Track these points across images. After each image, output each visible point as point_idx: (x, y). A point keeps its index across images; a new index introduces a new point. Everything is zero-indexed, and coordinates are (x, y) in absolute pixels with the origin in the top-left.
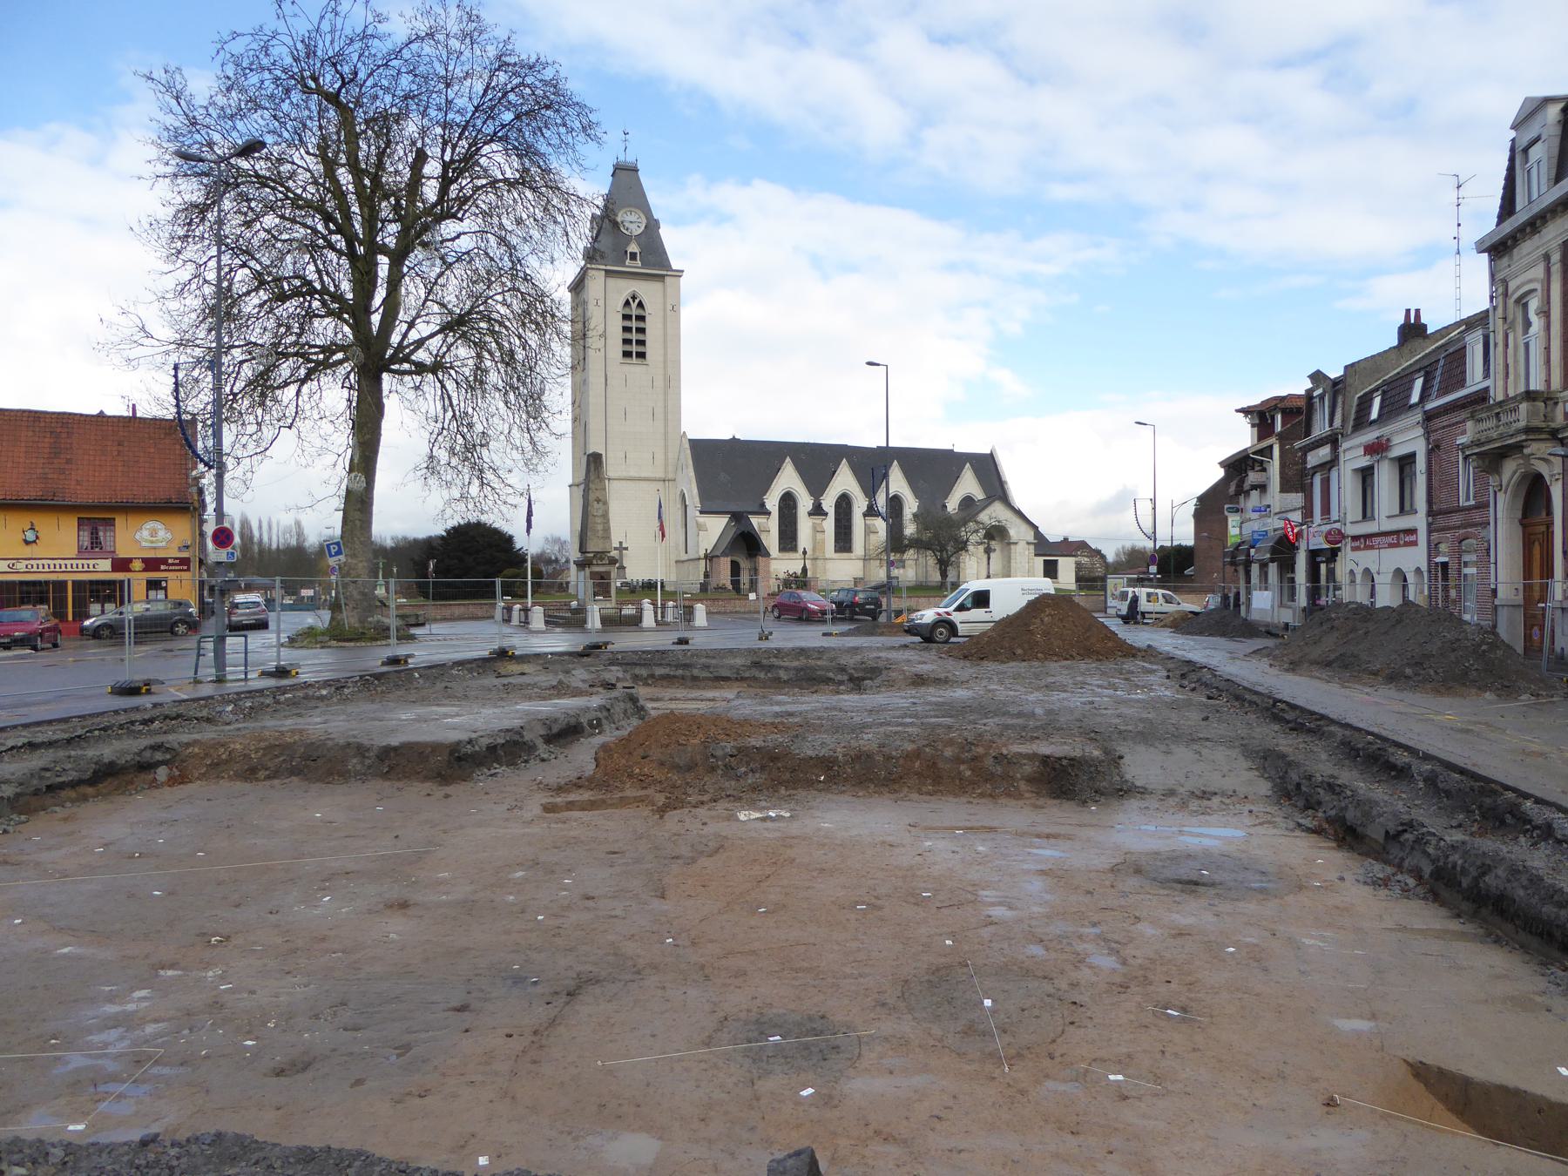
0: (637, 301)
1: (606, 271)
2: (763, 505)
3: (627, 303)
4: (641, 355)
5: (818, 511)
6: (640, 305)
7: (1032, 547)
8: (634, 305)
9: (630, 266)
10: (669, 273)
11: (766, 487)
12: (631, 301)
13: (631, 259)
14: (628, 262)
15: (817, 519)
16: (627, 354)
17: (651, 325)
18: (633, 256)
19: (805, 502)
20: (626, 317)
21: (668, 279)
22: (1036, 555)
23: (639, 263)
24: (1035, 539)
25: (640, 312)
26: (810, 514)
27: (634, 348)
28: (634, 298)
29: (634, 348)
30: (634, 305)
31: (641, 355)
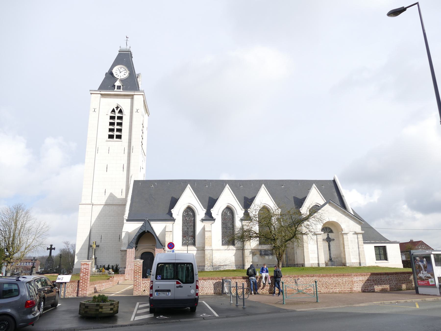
0: (119, 109)
1: (101, 94)
2: (171, 215)
3: (113, 111)
4: (119, 137)
5: (209, 217)
6: (121, 112)
7: (360, 236)
8: (117, 111)
9: (116, 91)
10: (135, 93)
11: (174, 202)
12: (115, 109)
13: (118, 89)
14: (116, 89)
15: (207, 224)
16: (111, 137)
17: (126, 121)
18: (119, 87)
19: (201, 213)
20: (112, 118)
21: (135, 96)
22: (364, 243)
23: (121, 90)
24: (362, 230)
25: (120, 115)
26: (203, 220)
27: (116, 133)
28: (117, 108)
29: (116, 133)
30: (117, 111)
31: (119, 137)
